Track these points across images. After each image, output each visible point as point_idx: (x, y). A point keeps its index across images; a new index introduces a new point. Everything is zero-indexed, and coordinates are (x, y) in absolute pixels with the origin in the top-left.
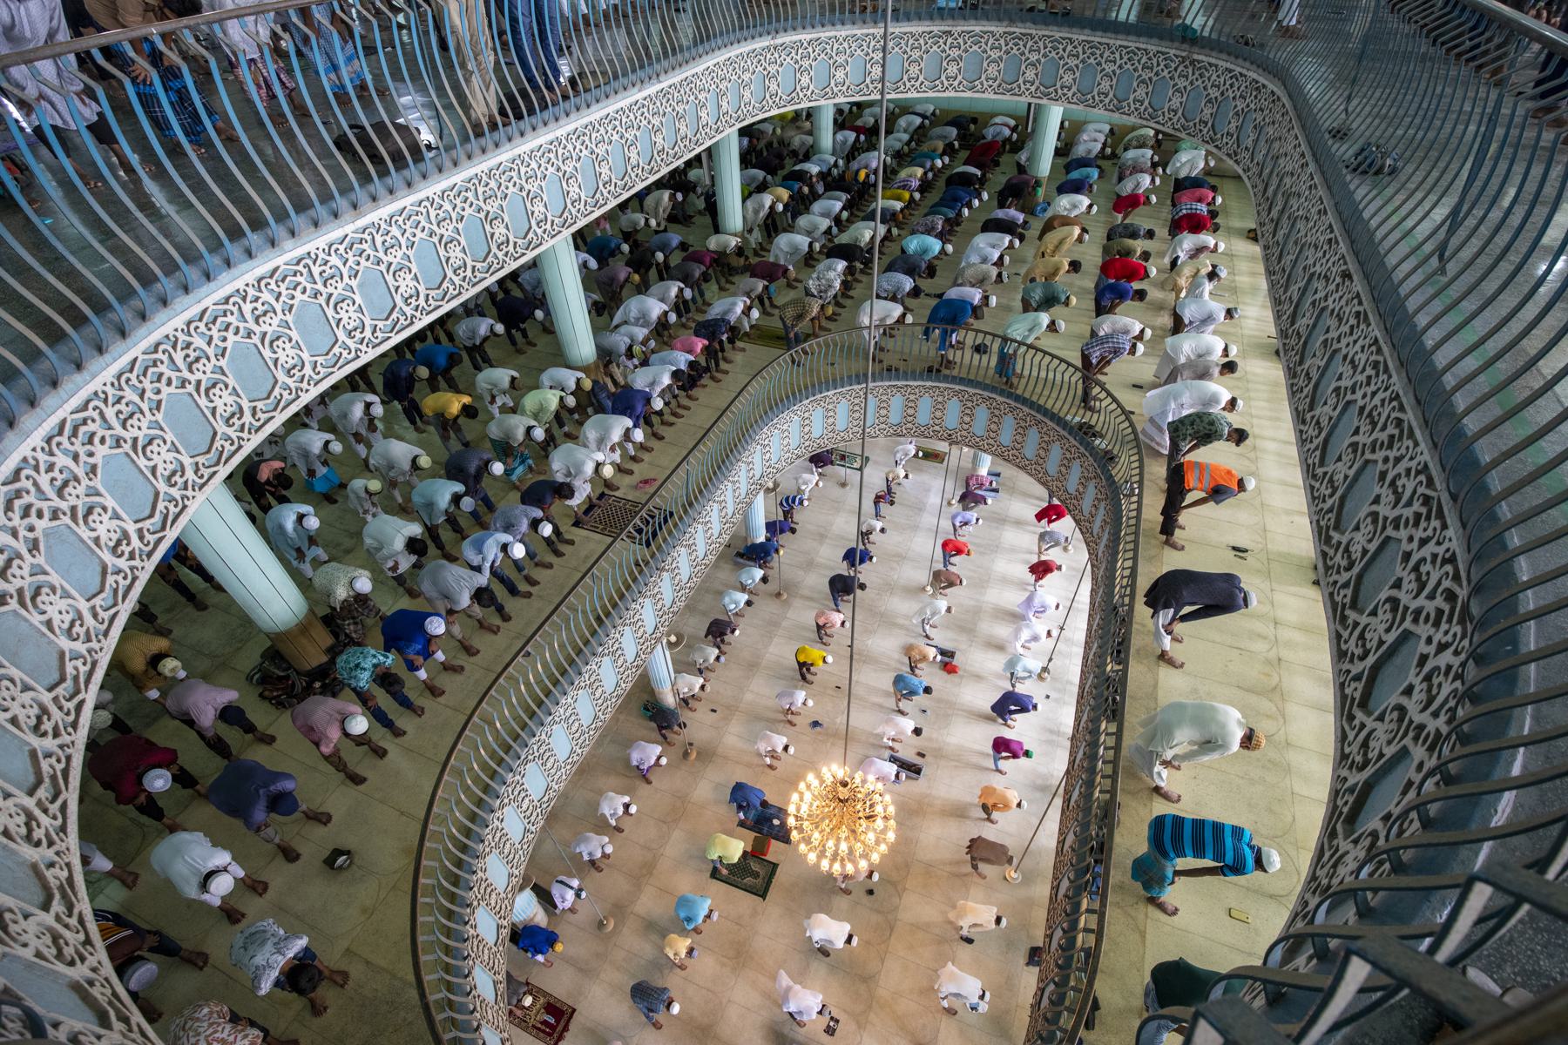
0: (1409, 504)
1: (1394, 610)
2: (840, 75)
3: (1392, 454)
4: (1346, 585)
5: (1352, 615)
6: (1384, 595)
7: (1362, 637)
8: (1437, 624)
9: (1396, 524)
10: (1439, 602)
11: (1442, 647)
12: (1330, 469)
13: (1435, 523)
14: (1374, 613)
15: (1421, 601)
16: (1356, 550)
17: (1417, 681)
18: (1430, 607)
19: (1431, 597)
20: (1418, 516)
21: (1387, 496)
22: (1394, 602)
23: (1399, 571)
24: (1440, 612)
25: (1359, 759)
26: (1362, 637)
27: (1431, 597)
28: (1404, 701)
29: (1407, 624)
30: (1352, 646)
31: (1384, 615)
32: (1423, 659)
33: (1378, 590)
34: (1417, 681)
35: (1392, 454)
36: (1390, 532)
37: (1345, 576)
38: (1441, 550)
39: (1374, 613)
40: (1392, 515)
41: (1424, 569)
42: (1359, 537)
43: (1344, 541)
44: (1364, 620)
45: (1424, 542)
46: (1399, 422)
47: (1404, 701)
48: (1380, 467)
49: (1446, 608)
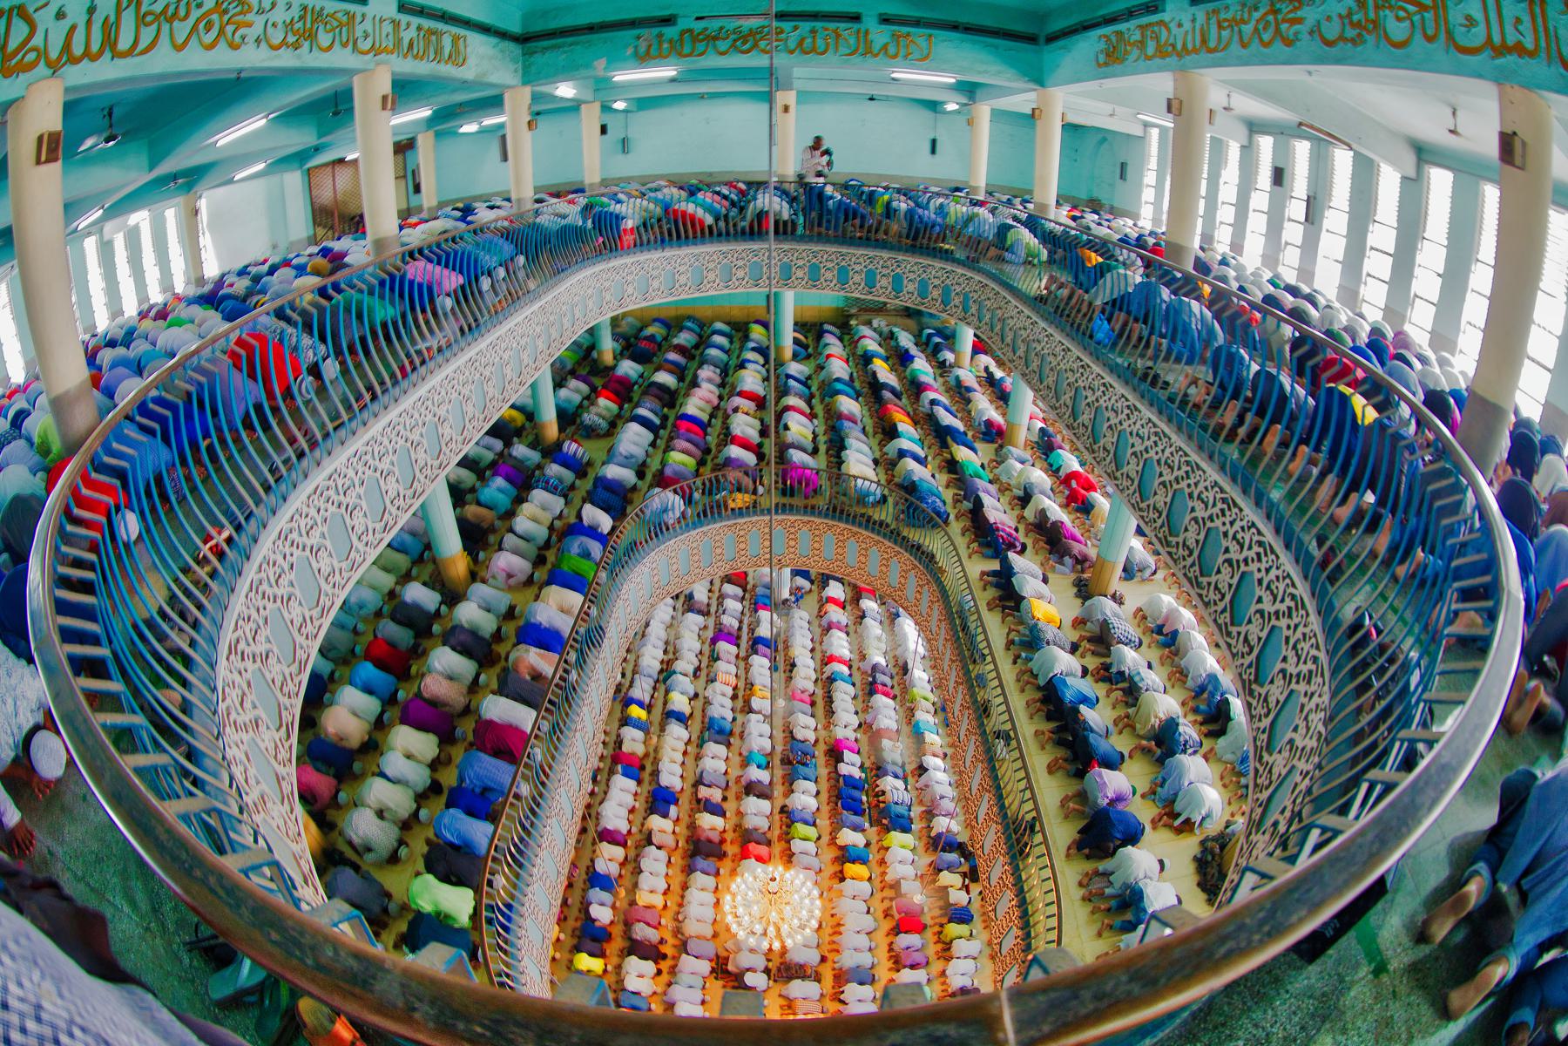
0: (1214, 505)
1: (1231, 565)
2: (656, 284)
3: (1191, 481)
4: (1193, 565)
5: (1204, 580)
6: (1221, 559)
7: (1216, 588)
8: (1259, 560)
9: (1211, 518)
10: (1256, 548)
11: (1267, 571)
12: (1151, 502)
13: (1235, 510)
14: (1219, 572)
15: (1245, 553)
16: (1191, 543)
17: (1262, 593)
18: (1252, 554)
19: (1250, 548)
20: (1222, 511)
21: (1199, 506)
22: (1229, 561)
23: (1225, 543)
24: (1258, 554)
25: (1246, 649)
26: (1216, 588)
27: (1250, 548)
28: (1260, 606)
29: (1243, 568)
30: (1212, 596)
31: (1226, 570)
32: (1260, 581)
33: (1215, 559)
34: (1262, 593)
35: (1191, 481)
36: (1209, 524)
37: (1190, 561)
38: (1244, 523)
39: (1219, 572)
40: (1206, 515)
41: (1239, 536)
42: (1188, 534)
43: (1180, 540)
44: (1213, 579)
45: (1232, 523)
46: (1188, 463)
47: (1260, 606)
48: (1187, 491)
49: (1261, 550)
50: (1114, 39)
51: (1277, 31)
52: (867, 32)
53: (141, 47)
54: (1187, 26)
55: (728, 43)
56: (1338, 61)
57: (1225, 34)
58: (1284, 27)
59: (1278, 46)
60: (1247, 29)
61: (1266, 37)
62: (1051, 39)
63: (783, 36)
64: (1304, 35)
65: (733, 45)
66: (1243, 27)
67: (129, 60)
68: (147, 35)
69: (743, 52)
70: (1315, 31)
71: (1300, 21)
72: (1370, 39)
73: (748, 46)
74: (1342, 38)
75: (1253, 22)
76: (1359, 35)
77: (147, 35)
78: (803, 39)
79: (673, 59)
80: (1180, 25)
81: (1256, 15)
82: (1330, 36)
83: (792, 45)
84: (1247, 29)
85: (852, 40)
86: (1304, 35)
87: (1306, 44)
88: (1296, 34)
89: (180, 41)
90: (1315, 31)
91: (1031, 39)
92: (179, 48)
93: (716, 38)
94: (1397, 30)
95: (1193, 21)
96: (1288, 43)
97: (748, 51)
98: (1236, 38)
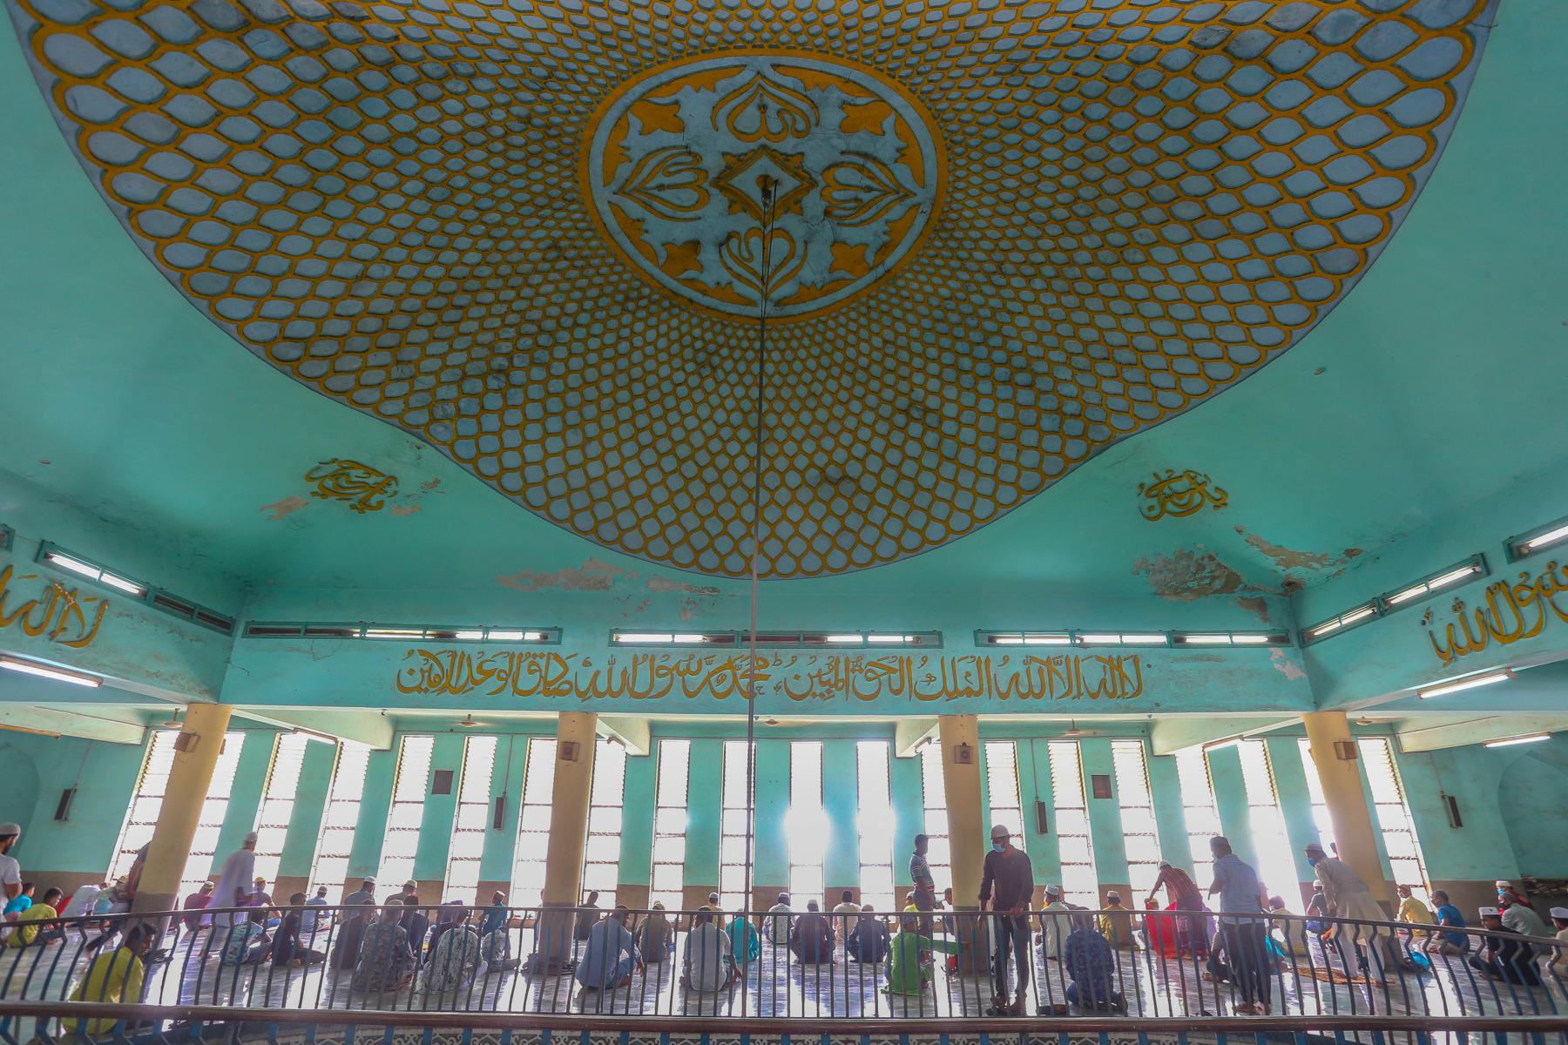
72: (840, 695)
76: (828, 691)
94: (866, 688)
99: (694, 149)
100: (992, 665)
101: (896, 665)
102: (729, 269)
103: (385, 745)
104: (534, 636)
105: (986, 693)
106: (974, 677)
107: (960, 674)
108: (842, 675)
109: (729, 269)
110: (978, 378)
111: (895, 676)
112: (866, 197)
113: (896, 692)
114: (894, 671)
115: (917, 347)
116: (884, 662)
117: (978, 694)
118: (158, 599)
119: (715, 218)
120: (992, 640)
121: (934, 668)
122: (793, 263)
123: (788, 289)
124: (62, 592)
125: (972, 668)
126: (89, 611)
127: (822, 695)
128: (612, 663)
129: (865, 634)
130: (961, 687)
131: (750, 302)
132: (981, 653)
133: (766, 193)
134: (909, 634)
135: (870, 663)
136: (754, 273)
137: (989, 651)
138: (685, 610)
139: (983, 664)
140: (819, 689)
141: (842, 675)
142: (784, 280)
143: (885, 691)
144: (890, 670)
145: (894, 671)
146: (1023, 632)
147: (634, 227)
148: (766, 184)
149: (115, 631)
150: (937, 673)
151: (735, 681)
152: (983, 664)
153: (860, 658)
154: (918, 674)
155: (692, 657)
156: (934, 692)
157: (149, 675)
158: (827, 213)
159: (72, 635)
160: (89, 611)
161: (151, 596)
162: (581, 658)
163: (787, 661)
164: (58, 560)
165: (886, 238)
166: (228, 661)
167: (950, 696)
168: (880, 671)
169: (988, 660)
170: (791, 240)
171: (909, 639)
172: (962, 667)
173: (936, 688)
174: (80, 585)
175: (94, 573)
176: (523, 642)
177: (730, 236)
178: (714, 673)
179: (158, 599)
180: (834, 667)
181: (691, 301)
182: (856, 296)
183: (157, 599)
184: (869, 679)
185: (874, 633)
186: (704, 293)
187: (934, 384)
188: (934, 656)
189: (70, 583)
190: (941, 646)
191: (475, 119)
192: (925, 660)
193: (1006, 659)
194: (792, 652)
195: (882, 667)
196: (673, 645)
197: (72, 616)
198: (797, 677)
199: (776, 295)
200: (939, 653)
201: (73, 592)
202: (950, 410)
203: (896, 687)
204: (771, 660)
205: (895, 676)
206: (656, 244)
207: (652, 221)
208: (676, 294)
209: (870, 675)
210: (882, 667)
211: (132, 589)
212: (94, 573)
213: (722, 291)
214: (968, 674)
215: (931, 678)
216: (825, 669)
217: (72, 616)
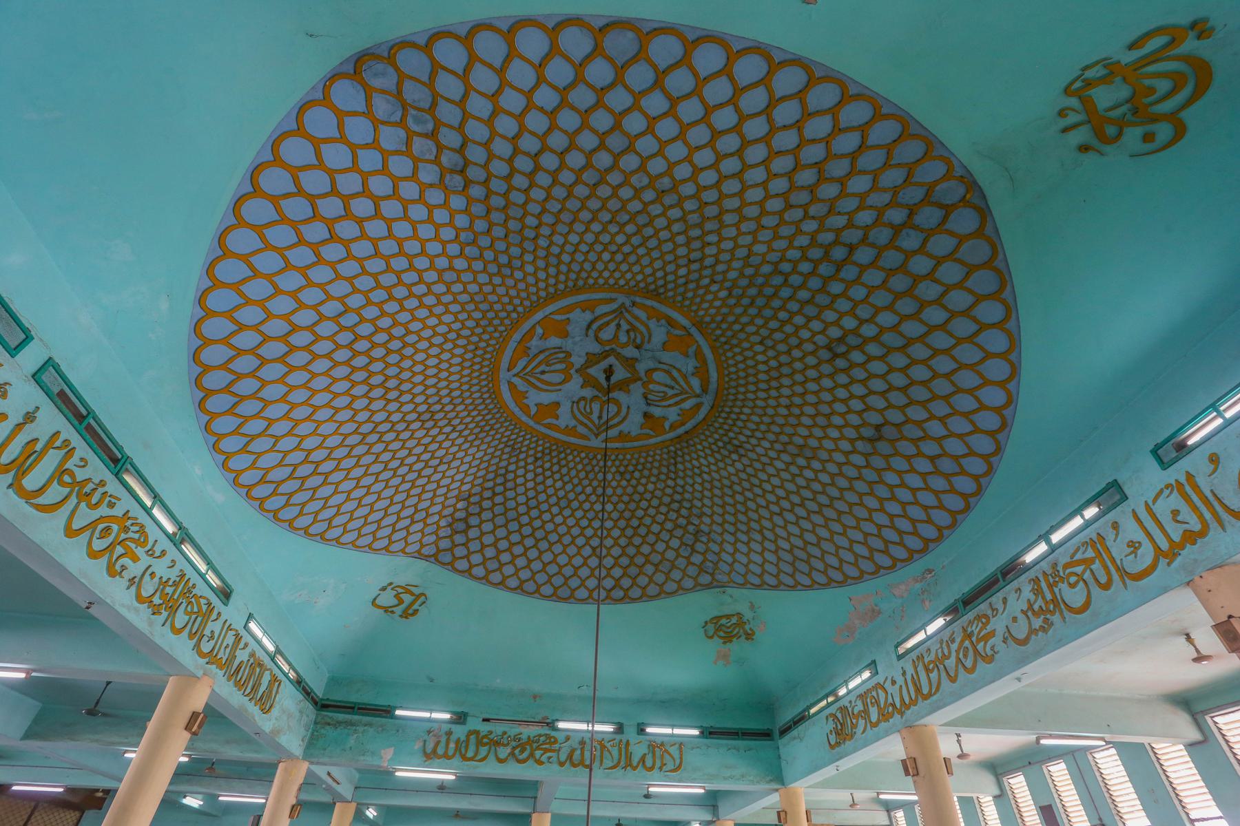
50: (839, 715)
51: (976, 651)
52: (628, 743)
53: (41, 500)
54: (900, 681)
55: (508, 750)
56: (1038, 654)
57: (934, 675)
58: (980, 647)
59: (981, 665)
60: (951, 663)
61: (969, 663)
62: (784, 731)
63: (557, 746)
64: (1001, 647)
65: (512, 754)
66: (947, 662)
67: (21, 503)
68: (55, 493)
69: (519, 761)
70: (1009, 637)
71: (992, 634)
73: (525, 755)
74: (1033, 631)
75: (954, 654)
76: (1046, 620)
77: (55, 493)
78: (573, 751)
79: (456, 761)
80: (894, 683)
81: (954, 646)
82: (1022, 636)
83: (563, 757)
84: (951, 663)
85: (615, 752)
86: (1001, 647)
87: (1006, 652)
88: (992, 648)
89: (75, 527)
90: (1009, 637)
91: (766, 735)
92: (70, 532)
93: (497, 744)
95: (904, 673)
96: (989, 659)
97: (524, 761)
98: (943, 674)
99: (575, 399)
100: (1202, 481)
101: (1090, 553)
102: (669, 406)
103: (997, 792)
104: (866, 674)
105: (1214, 525)
106: (1186, 513)
107: (1166, 520)
108: (1049, 596)
109: (669, 406)
110: (823, 290)
111: (1096, 566)
112: (625, 326)
113: (1106, 587)
114: (1092, 561)
115: (773, 324)
116: (1079, 556)
117: (1203, 533)
118: (711, 733)
119: (632, 400)
120: (1182, 447)
121: (1131, 531)
122: (675, 374)
123: (696, 383)
124: (657, 746)
125: (1175, 501)
126: (674, 751)
127: (1042, 629)
128: (904, 673)
129: (1045, 537)
130: (1176, 537)
131: (698, 406)
132: (1176, 473)
133: (608, 379)
134: (1088, 504)
135: (1066, 566)
136: (676, 395)
137: (1185, 464)
138: (923, 601)
139: (1187, 488)
140: (1037, 623)
141: (1049, 596)
142: (687, 383)
143: (1096, 591)
144: (1087, 562)
145: (1092, 561)
146: (1214, 406)
147: (622, 437)
148: (609, 372)
149: (691, 758)
150: (1139, 536)
151: (976, 651)
152: (1187, 488)
153: (1055, 565)
154: (1118, 550)
155: (941, 642)
156: (1148, 561)
157: (725, 779)
158: (638, 347)
159: (670, 766)
160: (674, 751)
161: (706, 733)
162: (889, 682)
163: (1000, 606)
164: (649, 730)
165: (663, 322)
166: (779, 757)
167: (1172, 553)
168: (1079, 569)
169: (1189, 476)
170: (656, 369)
171: (1091, 512)
172: (1163, 508)
173: (1146, 554)
174: (665, 739)
175: (668, 731)
176: (864, 682)
177: (646, 398)
178: (959, 649)
179: (711, 733)
180: (1037, 591)
181: (686, 432)
182: (713, 348)
183: (709, 733)
184: (1072, 586)
185: (1054, 529)
186: (683, 424)
187: (816, 325)
188: (1121, 514)
189: (659, 740)
190: (1125, 498)
191: (530, 476)
192: (1115, 526)
193: (1214, 459)
194: (1000, 595)
195: (1079, 563)
196: (929, 638)
197: (667, 756)
198: (1015, 619)
199: (698, 391)
200: (1125, 508)
201: (662, 744)
202: (850, 323)
203: (1103, 580)
204: (989, 612)
205: (1096, 566)
206: (639, 432)
207: (624, 427)
208: (679, 437)
209: (1073, 579)
210: (1079, 563)
211: (696, 732)
212: (668, 731)
213: (685, 416)
214: (1175, 513)
215: (1134, 546)
216: (1032, 597)
217: (667, 756)
